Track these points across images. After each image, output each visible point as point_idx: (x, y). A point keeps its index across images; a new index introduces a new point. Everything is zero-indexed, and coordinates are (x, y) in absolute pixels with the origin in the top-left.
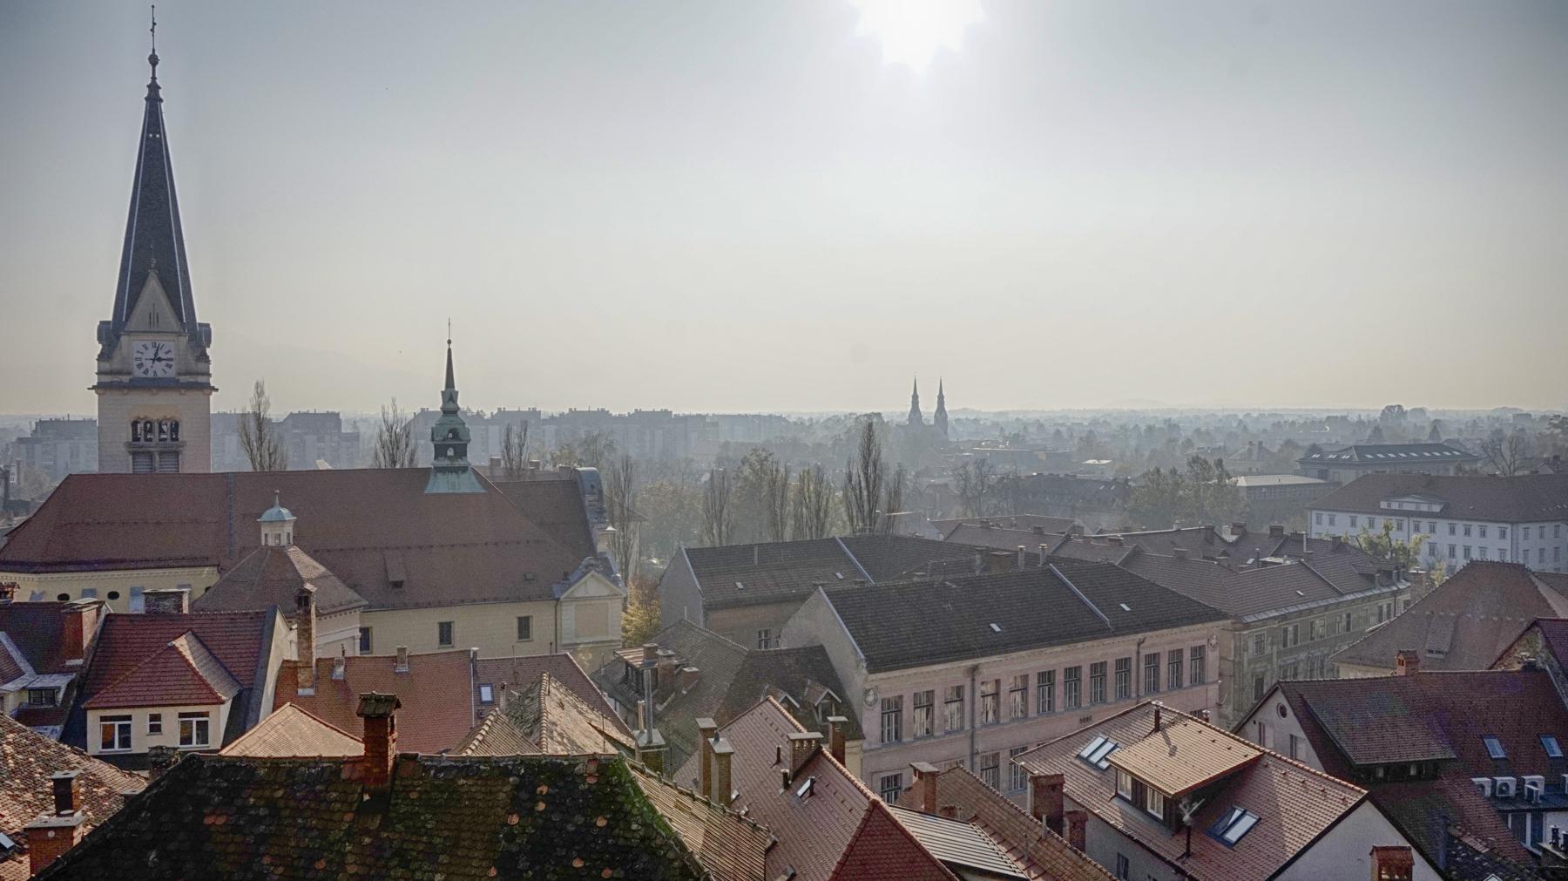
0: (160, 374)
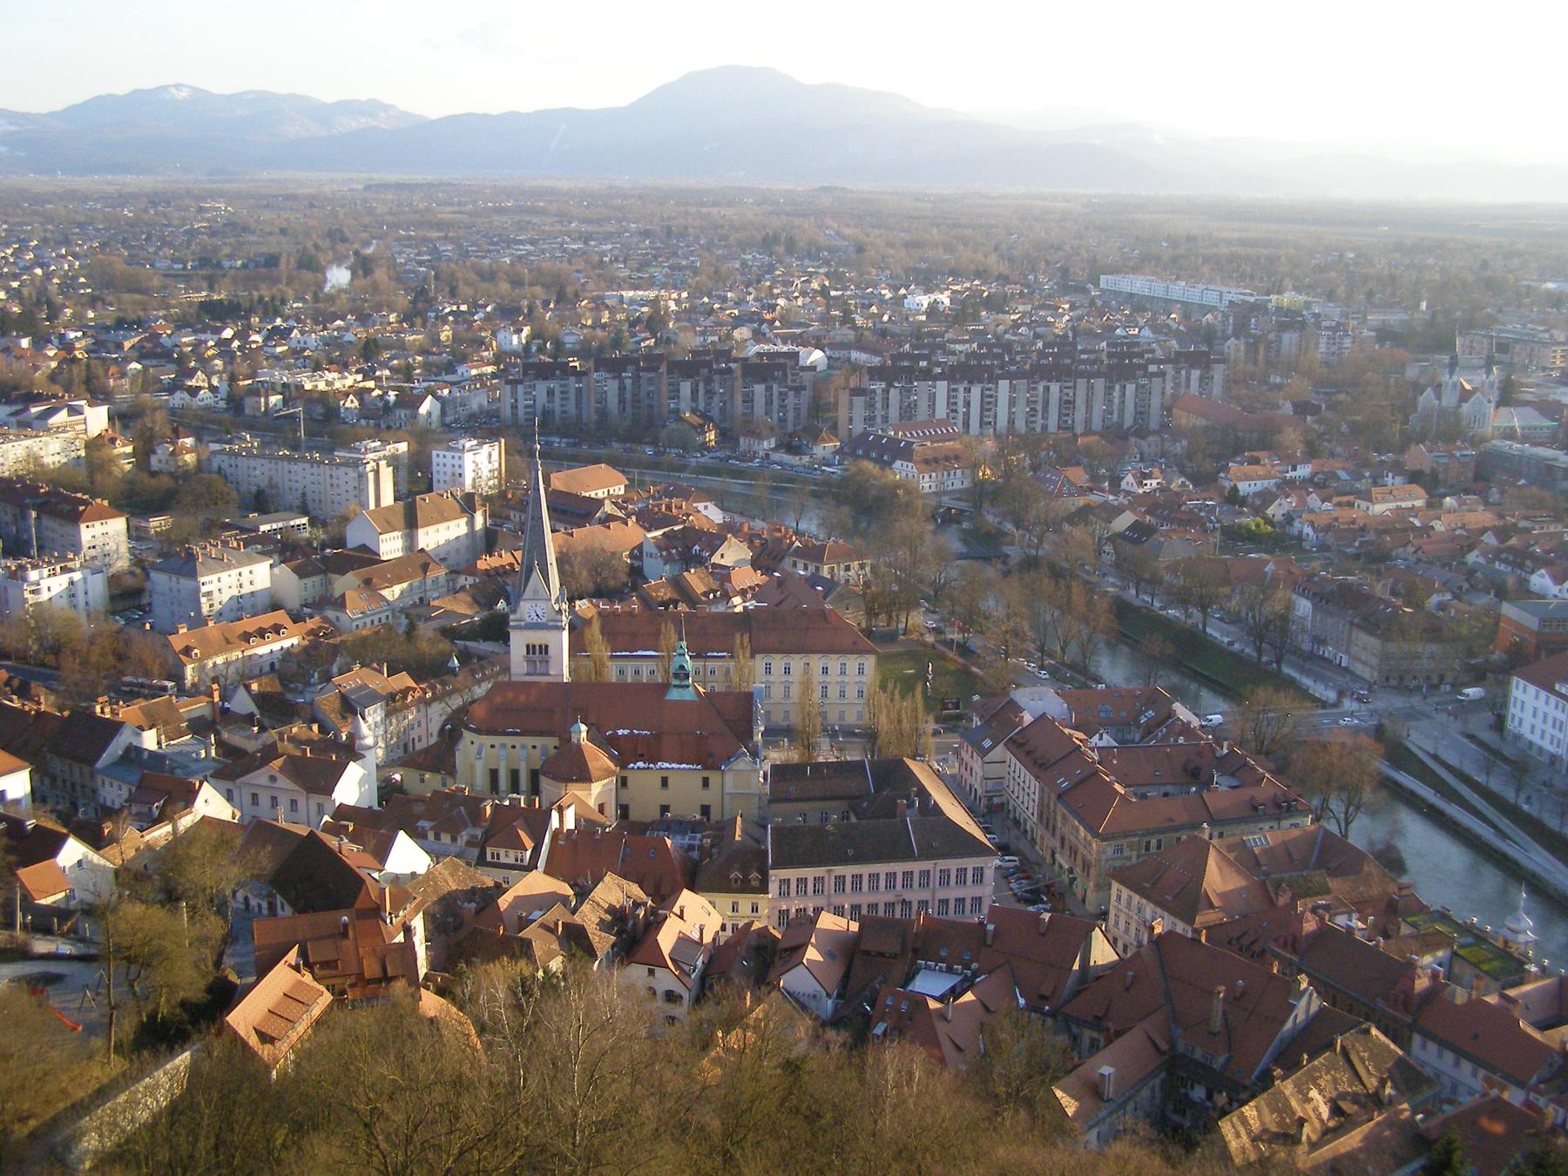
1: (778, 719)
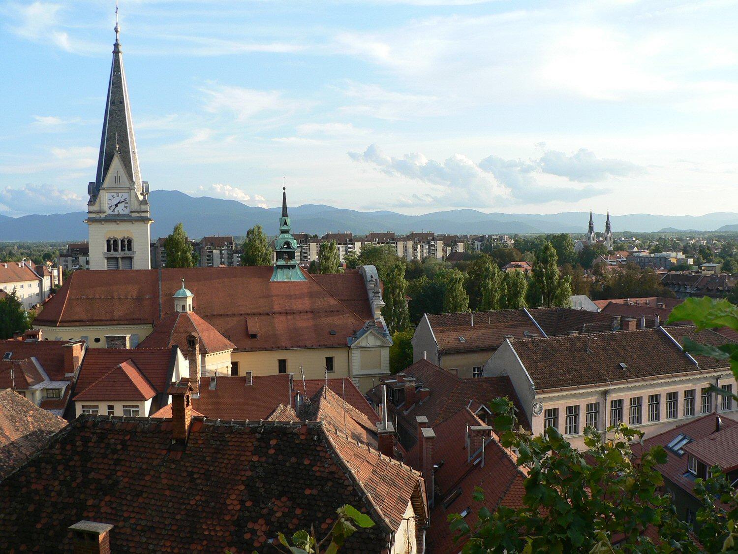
0: (121, 212)
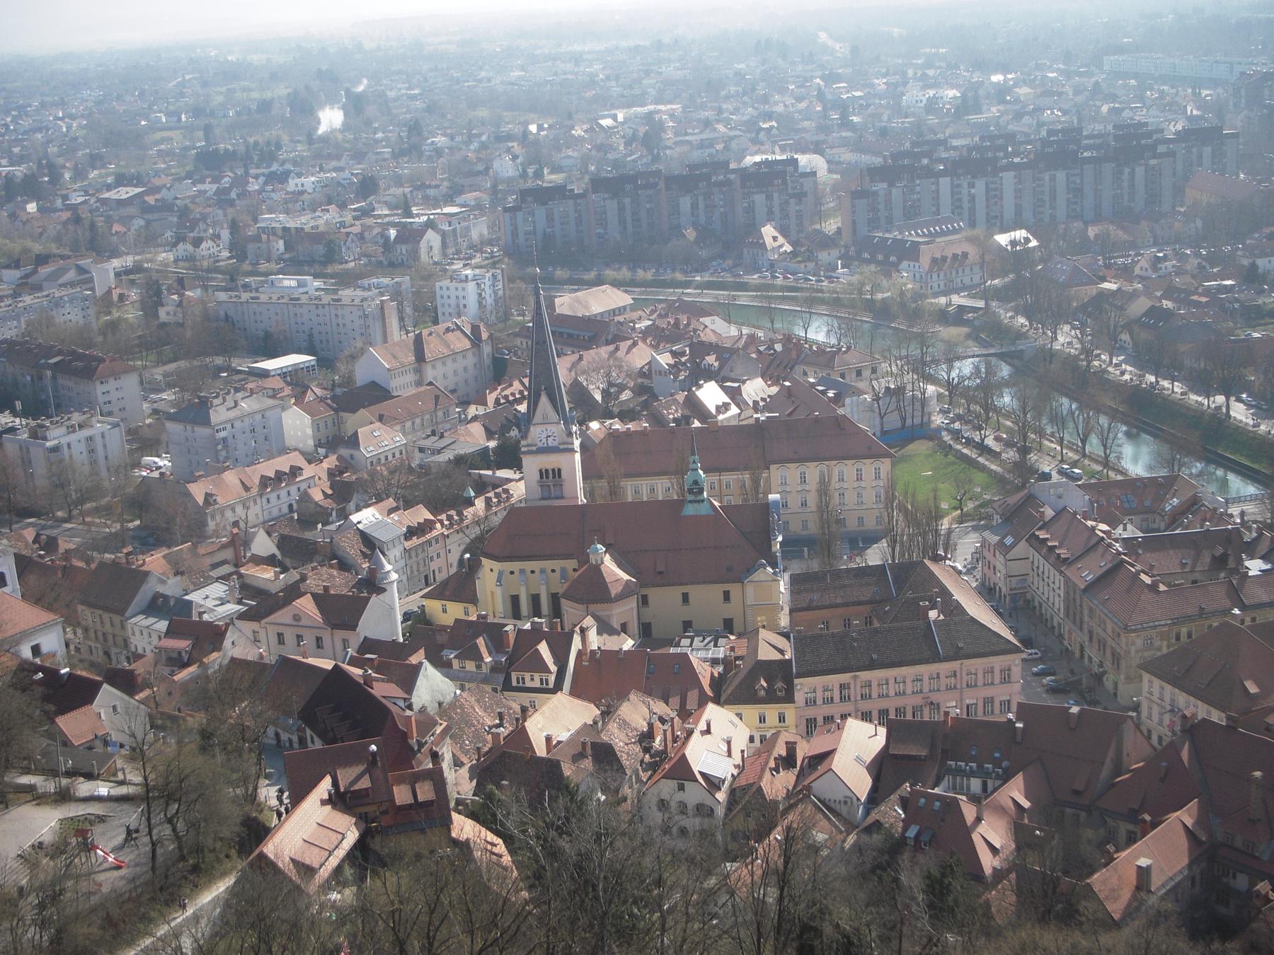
0: (550, 445)
1: (795, 527)
